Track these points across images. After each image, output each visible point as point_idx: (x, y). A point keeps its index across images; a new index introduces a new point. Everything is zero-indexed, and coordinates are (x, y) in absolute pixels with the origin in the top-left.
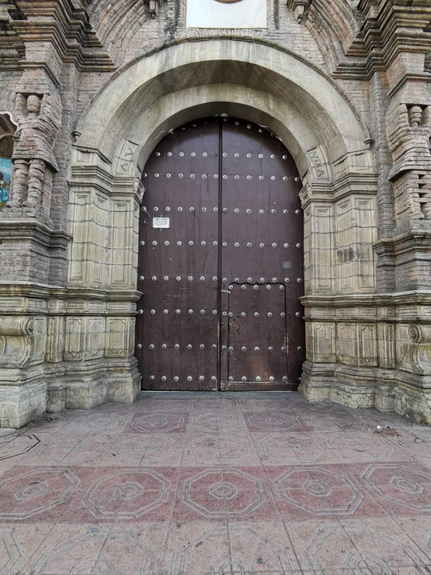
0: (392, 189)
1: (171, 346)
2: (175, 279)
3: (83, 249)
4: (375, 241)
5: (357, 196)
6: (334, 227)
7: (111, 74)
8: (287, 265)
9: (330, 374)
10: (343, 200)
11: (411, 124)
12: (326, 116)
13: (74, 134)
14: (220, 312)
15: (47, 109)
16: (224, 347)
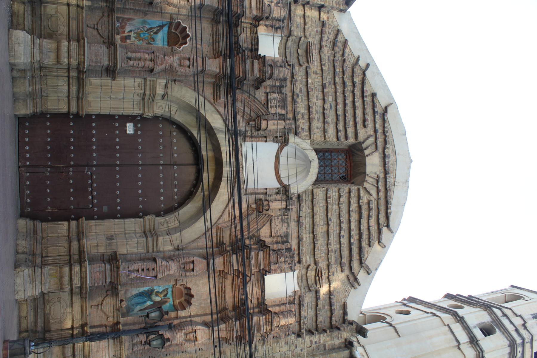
0: (149, 259)
1: (48, 135)
2: (93, 137)
3: (108, 86)
4: (118, 253)
5: (145, 242)
6: (129, 233)
7: (212, 101)
8: (105, 209)
9: (35, 232)
10: (144, 235)
11: (184, 264)
12: (193, 223)
13: (175, 81)
14: (72, 166)
15: (182, 70)
16: (49, 169)
